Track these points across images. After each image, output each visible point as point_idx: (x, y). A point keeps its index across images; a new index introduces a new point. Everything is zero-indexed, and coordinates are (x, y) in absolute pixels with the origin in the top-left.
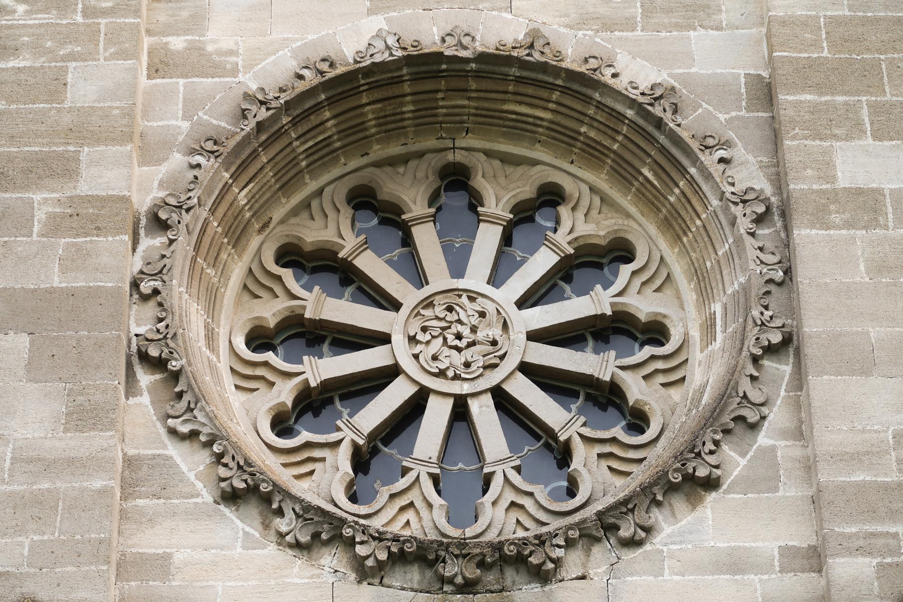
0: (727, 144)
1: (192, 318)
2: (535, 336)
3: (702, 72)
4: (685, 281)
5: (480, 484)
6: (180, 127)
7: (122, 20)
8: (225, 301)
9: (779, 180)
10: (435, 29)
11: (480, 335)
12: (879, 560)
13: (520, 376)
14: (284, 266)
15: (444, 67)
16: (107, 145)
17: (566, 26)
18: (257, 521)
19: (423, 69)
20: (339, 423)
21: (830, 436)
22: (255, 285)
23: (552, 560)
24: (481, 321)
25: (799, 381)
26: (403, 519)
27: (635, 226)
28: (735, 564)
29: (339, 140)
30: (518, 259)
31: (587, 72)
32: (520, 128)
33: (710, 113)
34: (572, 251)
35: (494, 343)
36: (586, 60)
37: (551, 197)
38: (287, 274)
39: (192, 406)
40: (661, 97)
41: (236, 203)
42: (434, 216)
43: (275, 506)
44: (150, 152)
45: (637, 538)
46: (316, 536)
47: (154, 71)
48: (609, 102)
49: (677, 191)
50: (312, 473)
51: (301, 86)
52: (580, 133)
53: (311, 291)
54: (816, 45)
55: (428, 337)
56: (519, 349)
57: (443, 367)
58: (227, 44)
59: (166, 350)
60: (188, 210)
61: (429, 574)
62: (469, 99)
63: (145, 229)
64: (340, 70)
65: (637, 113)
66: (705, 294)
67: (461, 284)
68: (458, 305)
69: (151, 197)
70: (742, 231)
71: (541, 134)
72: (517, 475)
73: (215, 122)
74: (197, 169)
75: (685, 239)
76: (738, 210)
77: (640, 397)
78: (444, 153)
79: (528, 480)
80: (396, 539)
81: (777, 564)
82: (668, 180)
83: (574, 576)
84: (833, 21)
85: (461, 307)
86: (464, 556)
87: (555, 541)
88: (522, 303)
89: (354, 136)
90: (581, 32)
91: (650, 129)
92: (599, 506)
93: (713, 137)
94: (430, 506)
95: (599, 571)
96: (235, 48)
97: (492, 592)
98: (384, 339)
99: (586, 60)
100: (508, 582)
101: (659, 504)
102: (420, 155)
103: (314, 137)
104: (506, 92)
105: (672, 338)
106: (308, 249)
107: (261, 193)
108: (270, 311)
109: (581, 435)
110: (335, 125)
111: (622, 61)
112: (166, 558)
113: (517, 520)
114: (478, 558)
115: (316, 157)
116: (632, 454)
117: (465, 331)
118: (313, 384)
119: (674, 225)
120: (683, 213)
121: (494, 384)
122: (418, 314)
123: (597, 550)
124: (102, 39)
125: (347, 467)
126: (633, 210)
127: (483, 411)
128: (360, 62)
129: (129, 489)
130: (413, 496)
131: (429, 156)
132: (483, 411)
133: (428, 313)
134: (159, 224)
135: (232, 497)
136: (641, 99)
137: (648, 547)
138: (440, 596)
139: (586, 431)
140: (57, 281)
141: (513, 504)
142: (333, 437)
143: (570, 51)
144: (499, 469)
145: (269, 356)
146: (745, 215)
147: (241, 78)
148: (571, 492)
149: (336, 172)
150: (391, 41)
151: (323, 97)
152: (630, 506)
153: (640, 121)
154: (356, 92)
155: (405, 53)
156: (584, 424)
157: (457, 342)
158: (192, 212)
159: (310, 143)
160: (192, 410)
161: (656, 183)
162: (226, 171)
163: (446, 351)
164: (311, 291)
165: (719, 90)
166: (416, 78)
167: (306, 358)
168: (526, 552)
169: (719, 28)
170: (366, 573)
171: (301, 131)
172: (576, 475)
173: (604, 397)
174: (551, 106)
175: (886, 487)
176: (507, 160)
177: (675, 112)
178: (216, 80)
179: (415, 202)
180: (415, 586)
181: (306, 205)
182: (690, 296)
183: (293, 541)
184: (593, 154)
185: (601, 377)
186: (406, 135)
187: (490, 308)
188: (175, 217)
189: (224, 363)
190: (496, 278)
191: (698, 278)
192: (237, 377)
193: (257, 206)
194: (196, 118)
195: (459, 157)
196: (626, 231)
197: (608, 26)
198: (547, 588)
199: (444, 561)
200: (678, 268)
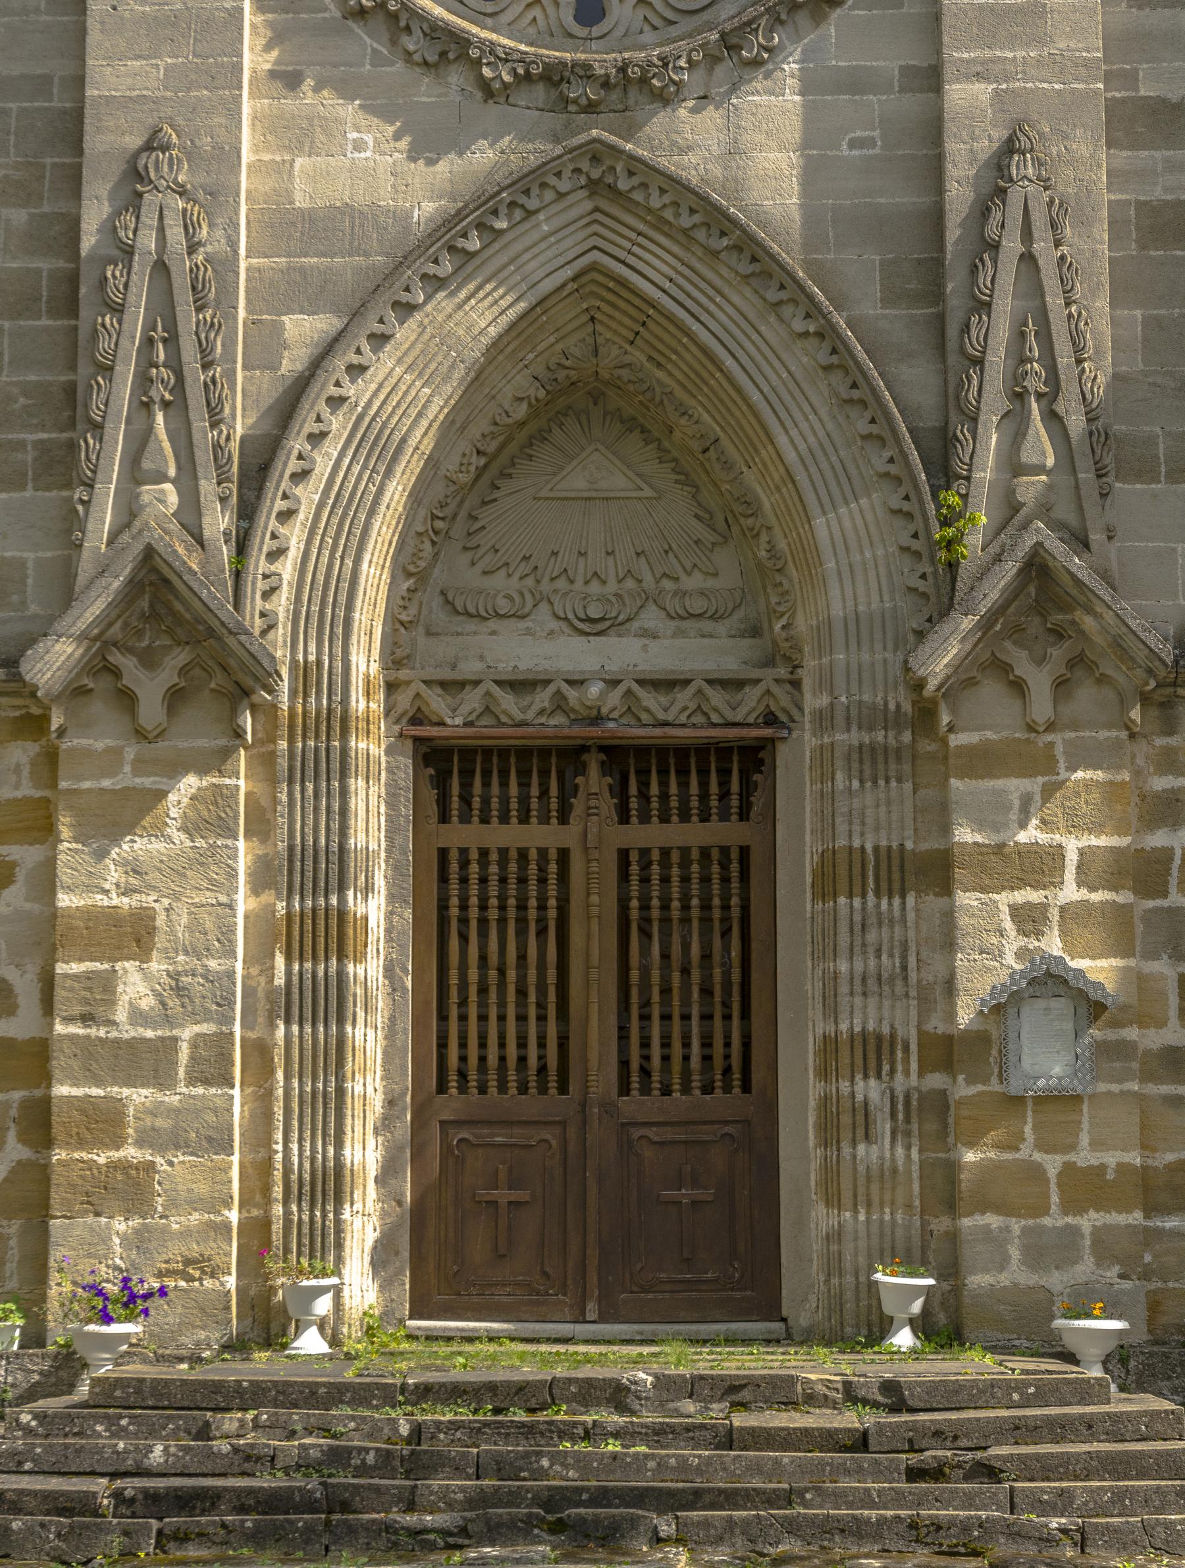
12: (994, 86)
18: (386, 36)
43: (402, 24)
46: (443, 54)
61: (554, 94)
81: (896, 83)
86: (589, 77)
100: (631, 102)
101: (782, 23)
180: (541, 106)
183: (420, 60)
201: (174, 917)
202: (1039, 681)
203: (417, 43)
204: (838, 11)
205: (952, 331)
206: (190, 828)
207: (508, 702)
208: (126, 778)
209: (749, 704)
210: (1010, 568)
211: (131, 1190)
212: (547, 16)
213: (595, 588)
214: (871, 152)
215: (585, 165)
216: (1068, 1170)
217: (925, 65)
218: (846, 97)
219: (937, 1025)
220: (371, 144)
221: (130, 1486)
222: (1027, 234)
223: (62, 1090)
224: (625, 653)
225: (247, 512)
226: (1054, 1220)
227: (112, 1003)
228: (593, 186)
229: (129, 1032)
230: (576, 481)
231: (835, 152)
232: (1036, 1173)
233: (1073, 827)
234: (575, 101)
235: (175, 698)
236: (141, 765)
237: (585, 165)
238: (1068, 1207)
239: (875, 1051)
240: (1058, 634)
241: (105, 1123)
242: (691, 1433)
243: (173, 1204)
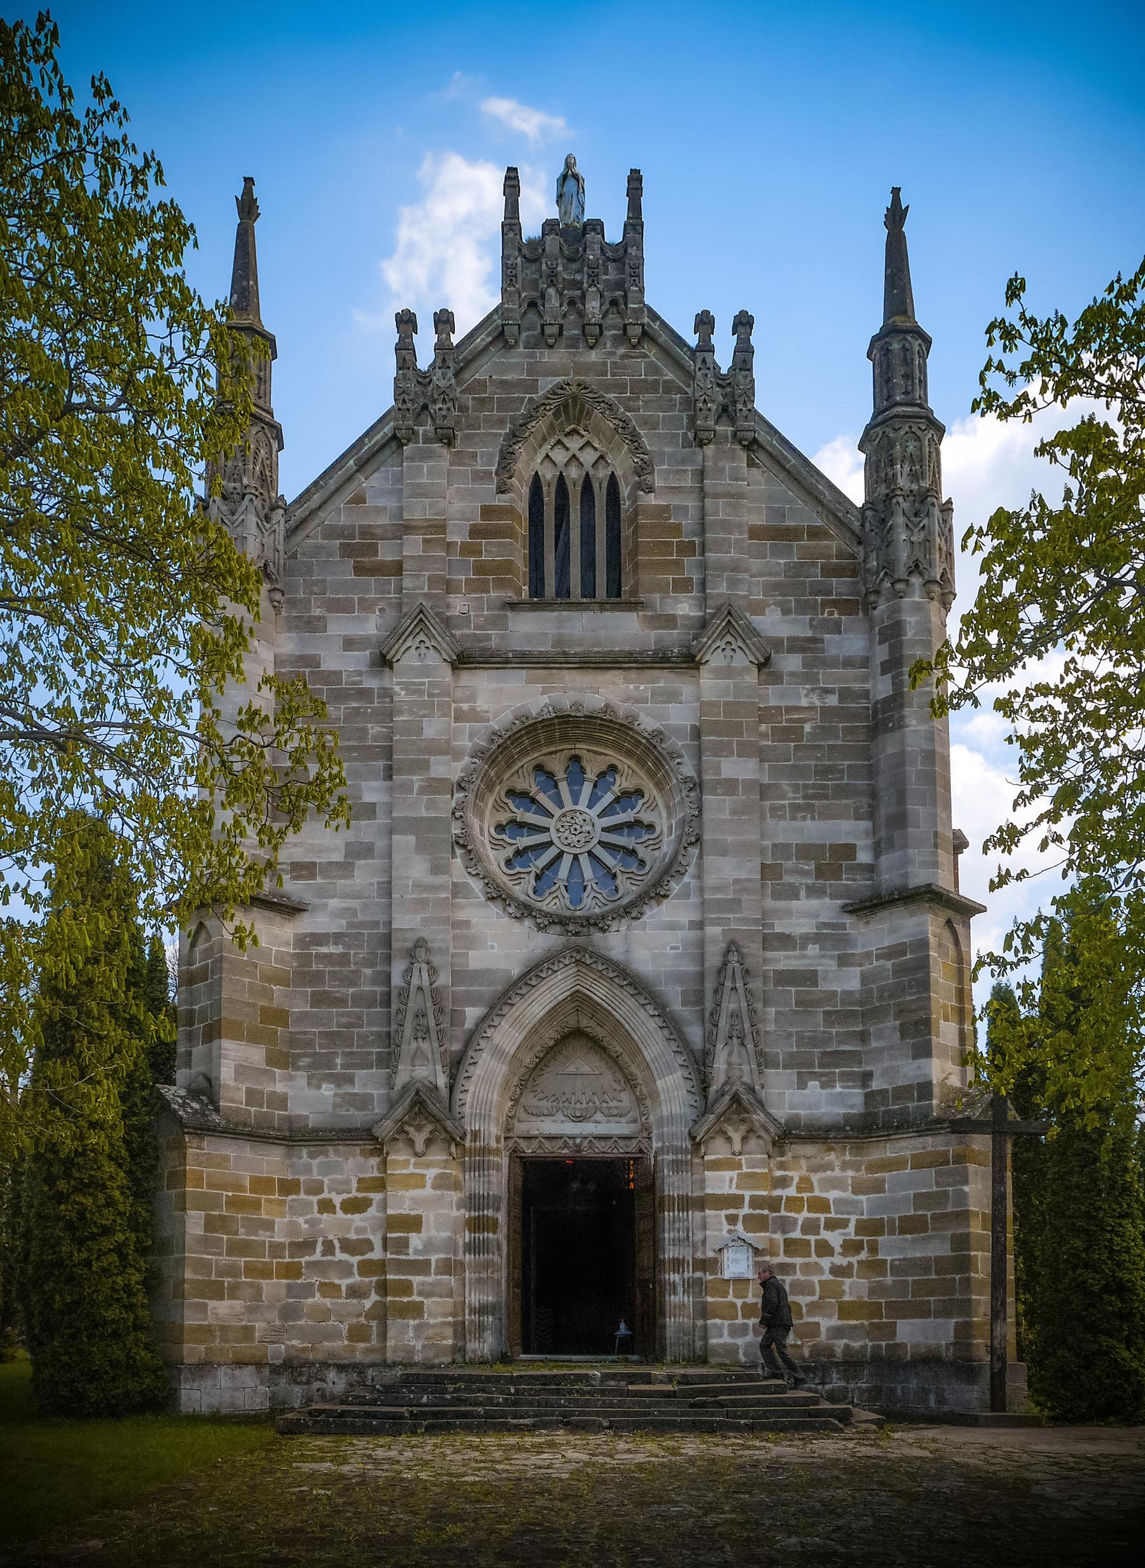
0: (680, 756)
1: (475, 823)
9: (700, 773)
21: (710, 880)
25: (701, 856)
28: (672, 926)
44: (456, 755)
47: (457, 720)
54: (718, 714)
56: (598, 835)
66: (669, 816)
84: (726, 703)
89: (536, 745)
92: (625, 901)
98: (548, 829)
108: (503, 818)
119: (659, 786)
127: (584, 860)
129: (455, 895)
132: (584, 860)
134: (461, 788)
135: (493, 899)
140: (424, 813)
148: (616, 890)
170: (540, 928)
175: (727, 901)
179: (560, 775)
182: (664, 815)
184: (629, 754)
189: (487, 841)
190: (590, 806)
197: (637, 701)
201: (429, 1217)
202: (737, 1137)
205: (707, 1015)
206: (434, 1187)
207: (548, 1144)
208: (411, 1170)
209: (633, 1145)
210: (727, 1097)
211: (416, 1310)
213: (578, 1106)
216: (745, 1304)
219: (699, 1255)
221: (415, 1410)
222: (734, 980)
223: (389, 1277)
224: (588, 1128)
225: (453, 1078)
226: (740, 1321)
227: (407, 1247)
228: (578, 962)
229: (412, 1257)
230: (571, 1069)
232: (733, 1306)
233: (747, 1188)
235: (429, 1142)
236: (416, 1165)
238: (744, 1317)
239: (678, 1264)
240: (743, 1121)
241: (406, 1288)
242: (612, 1392)
243: (430, 1315)
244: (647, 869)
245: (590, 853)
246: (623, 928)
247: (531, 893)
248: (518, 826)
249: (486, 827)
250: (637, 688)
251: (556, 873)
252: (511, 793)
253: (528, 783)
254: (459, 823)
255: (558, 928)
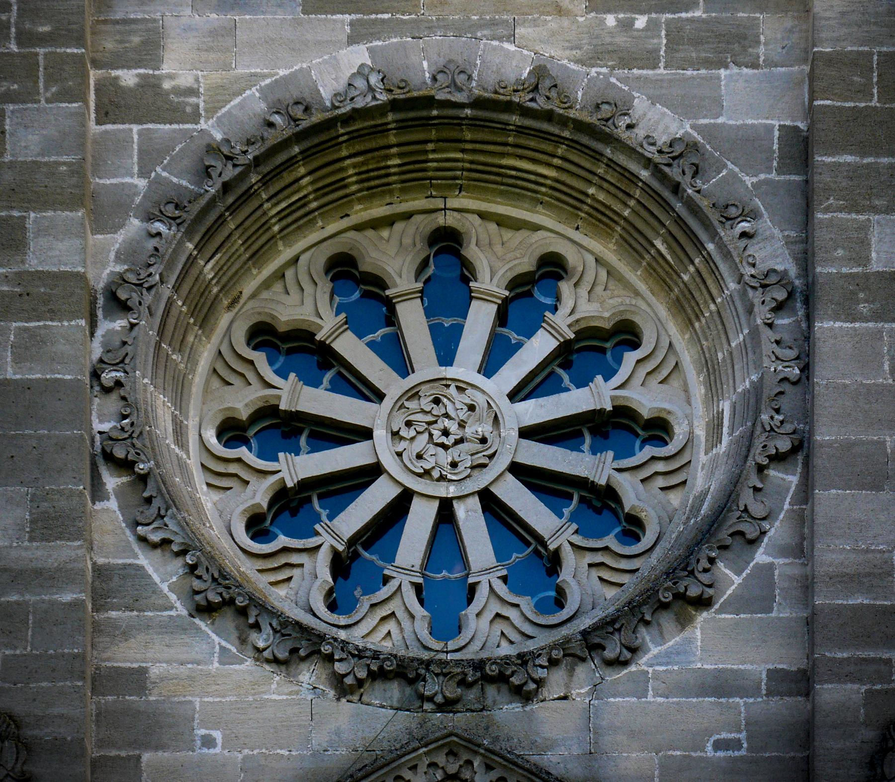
2: (526, 433)
3: (731, 122)
4: (694, 372)
5: (464, 594)
6: (136, 186)
7: (63, 50)
8: (194, 389)
10: (425, 64)
11: (469, 431)
13: (510, 477)
14: (255, 348)
15: (435, 113)
16: (55, 210)
17: (577, 62)
18: (234, 634)
19: (412, 114)
20: (317, 527)
22: (224, 373)
23: (534, 681)
24: (470, 416)
26: (384, 630)
27: (644, 306)
29: (315, 199)
30: (513, 342)
31: (598, 123)
32: (519, 187)
33: (734, 175)
34: (572, 336)
35: (483, 440)
36: (598, 106)
37: (552, 268)
38: (260, 358)
39: (162, 512)
40: (681, 155)
41: (201, 277)
42: (421, 292)
45: (622, 659)
46: (294, 651)
48: (622, 159)
49: (691, 269)
50: (290, 579)
51: (273, 138)
52: (587, 195)
53: (286, 378)
55: (413, 433)
57: (427, 466)
58: (186, 80)
59: (132, 451)
60: (149, 289)
62: (463, 151)
63: (103, 311)
64: (317, 118)
65: (653, 175)
67: (450, 372)
68: (446, 397)
69: (108, 271)
70: (759, 321)
71: (544, 194)
72: (503, 585)
73: (175, 180)
74: (157, 239)
75: (697, 325)
76: (756, 297)
77: (637, 503)
78: (434, 215)
79: (513, 590)
80: (376, 655)
81: (764, 687)
82: (682, 256)
83: (556, 696)
85: (449, 399)
87: (538, 662)
88: (514, 396)
89: (333, 196)
90: (594, 70)
91: (667, 194)
92: (585, 622)
93: (736, 206)
94: (412, 617)
95: (582, 691)
96: (196, 86)
97: (473, 711)
98: (366, 434)
99: (598, 106)
100: (489, 702)
101: (647, 623)
102: (407, 216)
103: (288, 197)
104: (506, 144)
105: (675, 438)
106: (282, 329)
107: (229, 264)
108: (243, 401)
109: (571, 544)
110: (312, 183)
111: (640, 104)
112: (143, 671)
113: (502, 633)
114: (460, 677)
115: (290, 220)
116: (624, 565)
117: (453, 427)
118: (290, 484)
119: (686, 308)
120: (697, 295)
121: (482, 486)
122: (402, 406)
123: (581, 671)
124: (41, 73)
125: (325, 575)
126: (642, 287)
127: (470, 517)
128: (338, 107)
130: (394, 606)
131: (417, 218)
132: (470, 517)
133: (412, 405)
136: (657, 158)
137: (633, 668)
138: (419, 715)
139: (578, 540)
141: (498, 615)
142: (312, 542)
143: (580, 94)
144: (484, 579)
145: (243, 452)
146: (763, 302)
147: (203, 125)
149: (314, 237)
150: (374, 79)
151: (297, 149)
152: (617, 626)
153: (656, 185)
154: (334, 143)
155: (391, 97)
156: (576, 532)
157: (444, 440)
158: (153, 291)
159: (283, 205)
160: (163, 517)
161: (669, 257)
162: (190, 241)
163: (432, 449)
164: (286, 378)
165: (746, 144)
166: (403, 126)
167: (281, 455)
168: (508, 673)
169: (755, 66)
171: (272, 190)
172: (564, 586)
173: (599, 501)
174: (556, 161)
176: (503, 222)
177: (695, 174)
178: (175, 126)
179: (402, 277)
180: (395, 704)
181: (280, 275)
182: (698, 391)
183: (271, 657)
184: (601, 219)
185: (596, 480)
186: (391, 192)
187: (480, 400)
188: (135, 297)
189: (193, 460)
191: (708, 370)
192: (208, 475)
193: (225, 279)
194: (153, 174)
195: (450, 220)
196: (633, 313)
197: (627, 60)
198: (528, 708)
199: (424, 680)
200: (687, 357)
203: (266, 640)
204: (705, 614)
212: (402, 630)
214: (737, 753)
215: (441, 759)
217: (794, 669)
218: (712, 699)
220: (219, 741)
231: (699, 754)
234: (430, 699)
237: (441, 759)
244: (647, 540)
245: (488, 499)
246: (580, 692)
247: (321, 608)
248: (284, 428)
249: (192, 423)
250: (626, 25)
251: (390, 557)
252: (263, 335)
253: (311, 306)
254: (112, 403)
255: (394, 691)
